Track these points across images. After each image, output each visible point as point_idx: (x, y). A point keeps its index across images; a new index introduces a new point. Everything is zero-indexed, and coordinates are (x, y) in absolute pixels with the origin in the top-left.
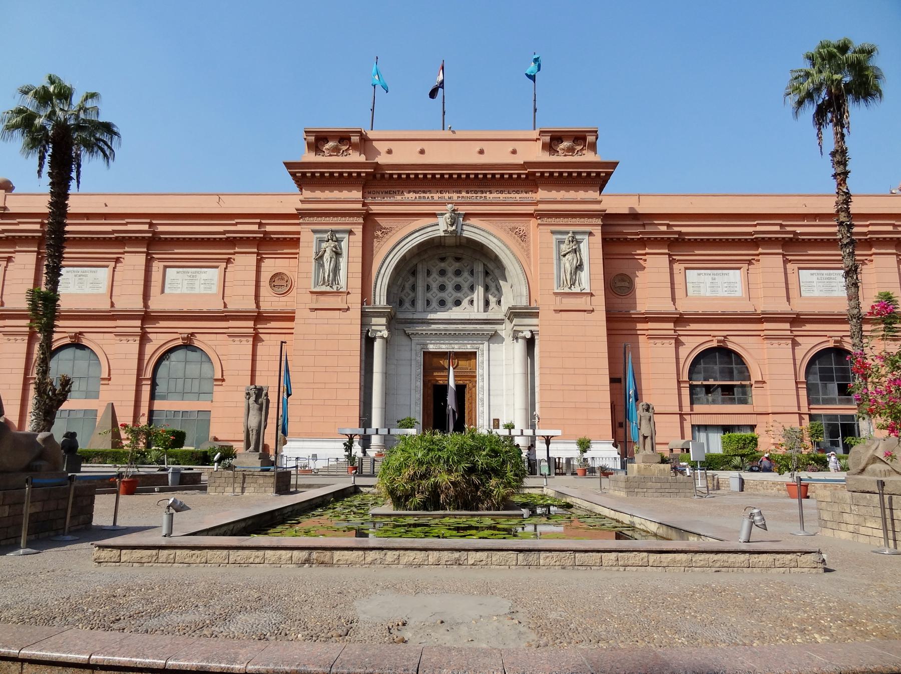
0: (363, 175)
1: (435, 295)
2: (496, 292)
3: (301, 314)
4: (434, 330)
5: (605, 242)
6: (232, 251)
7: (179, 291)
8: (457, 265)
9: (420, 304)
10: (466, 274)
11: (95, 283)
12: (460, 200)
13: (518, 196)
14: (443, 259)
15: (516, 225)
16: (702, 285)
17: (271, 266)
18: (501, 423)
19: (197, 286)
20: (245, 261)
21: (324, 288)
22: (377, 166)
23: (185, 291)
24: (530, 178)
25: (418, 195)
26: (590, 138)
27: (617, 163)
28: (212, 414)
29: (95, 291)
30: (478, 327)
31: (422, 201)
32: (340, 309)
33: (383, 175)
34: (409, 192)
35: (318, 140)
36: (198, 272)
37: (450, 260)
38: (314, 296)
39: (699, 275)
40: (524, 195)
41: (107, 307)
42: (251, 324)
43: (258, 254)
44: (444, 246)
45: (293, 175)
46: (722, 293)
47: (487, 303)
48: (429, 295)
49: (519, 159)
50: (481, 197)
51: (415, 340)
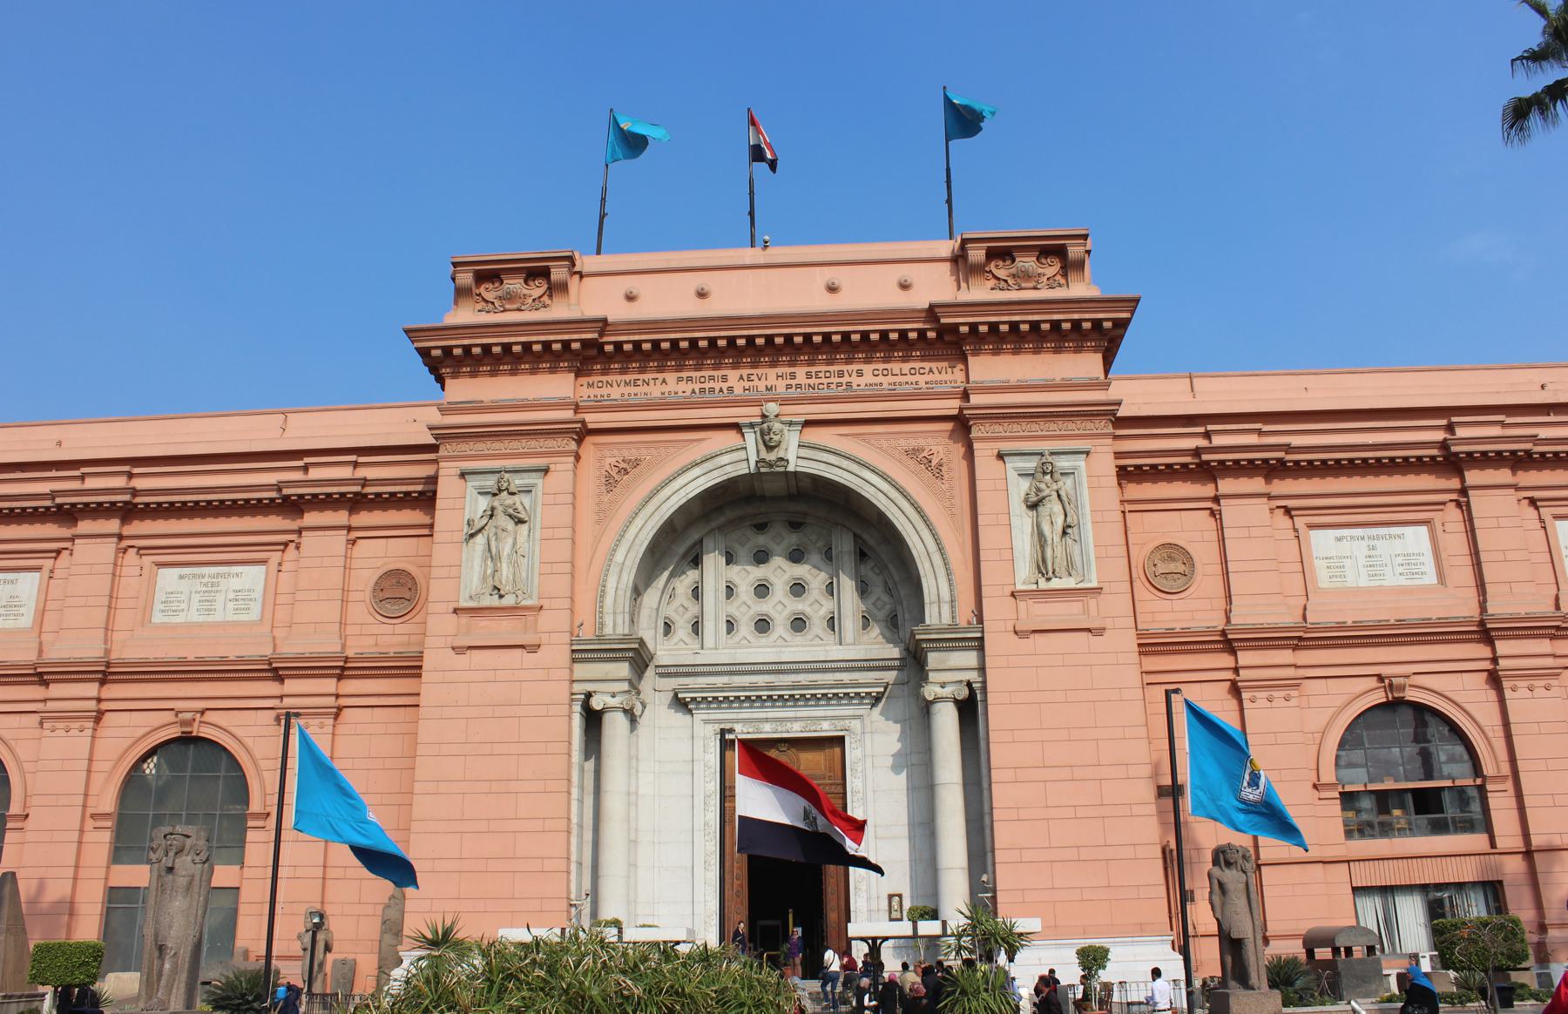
0: (576, 346)
1: (746, 607)
2: (886, 598)
4: (744, 689)
6: (294, 525)
7: (180, 619)
8: (792, 539)
11: (12, 605)
12: (793, 393)
13: (922, 379)
14: (761, 527)
15: (921, 442)
16: (1347, 562)
17: (378, 556)
18: (907, 904)
19: (219, 605)
21: (488, 601)
22: (603, 324)
23: (194, 617)
24: (947, 338)
25: (697, 387)
27: (1137, 301)
28: (244, 895)
29: (10, 624)
30: (846, 677)
31: (708, 397)
32: (522, 647)
33: (618, 346)
34: (680, 379)
36: (223, 576)
38: (464, 619)
39: (1339, 539)
40: (937, 377)
41: (32, 657)
42: (329, 685)
44: (763, 498)
45: (424, 353)
46: (1392, 579)
48: (733, 609)
49: (920, 299)
50: (839, 385)
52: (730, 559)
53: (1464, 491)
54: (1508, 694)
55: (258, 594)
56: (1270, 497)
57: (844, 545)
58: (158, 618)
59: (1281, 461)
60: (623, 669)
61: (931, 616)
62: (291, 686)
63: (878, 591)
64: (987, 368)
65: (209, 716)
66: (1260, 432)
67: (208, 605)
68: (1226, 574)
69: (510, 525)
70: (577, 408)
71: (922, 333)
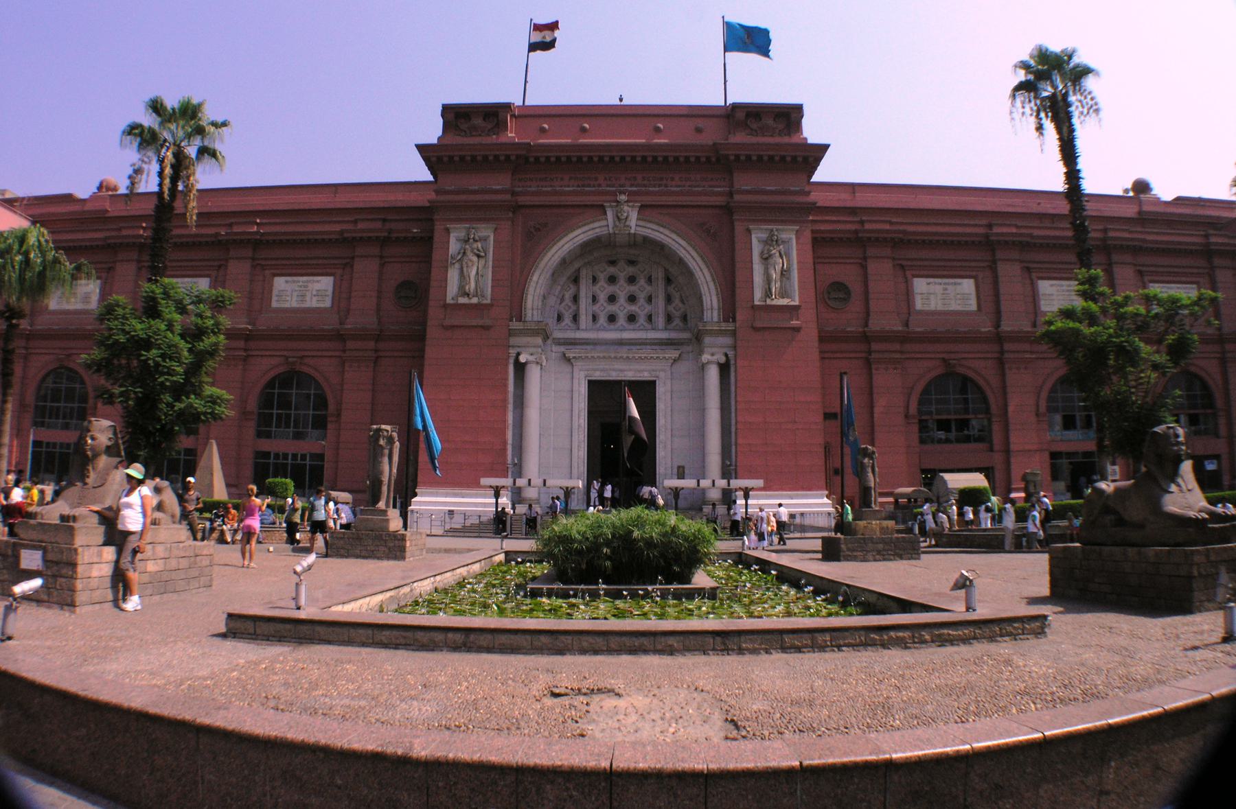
1: (604, 308)
2: (681, 305)
3: (432, 332)
5: (815, 241)
7: (287, 305)
8: (631, 270)
9: (584, 320)
10: (642, 282)
14: (613, 263)
19: (308, 298)
20: (366, 268)
21: (462, 300)
23: (295, 305)
26: (794, 116)
33: (537, 159)
34: (571, 178)
35: (455, 116)
37: (622, 264)
42: (372, 344)
43: (381, 257)
46: (954, 306)
47: (669, 318)
48: (596, 308)
51: (578, 365)
52: (595, 280)
53: (994, 262)
54: (1007, 371)
55: (330, 292)
56: (894, 259)
57: (659, 274)
58: (274, 304)
59: (902, 240)
60: (539, 340)
61: (707, 316)
62: (350, 344)
63: (677, 302)
64: (745, 182)
65: (306, 361)
66: (891, 223)
67: (302, 297)
68: (867, 300)
69: (475, 259)
70: (513, 194)
71: (708, 158)
